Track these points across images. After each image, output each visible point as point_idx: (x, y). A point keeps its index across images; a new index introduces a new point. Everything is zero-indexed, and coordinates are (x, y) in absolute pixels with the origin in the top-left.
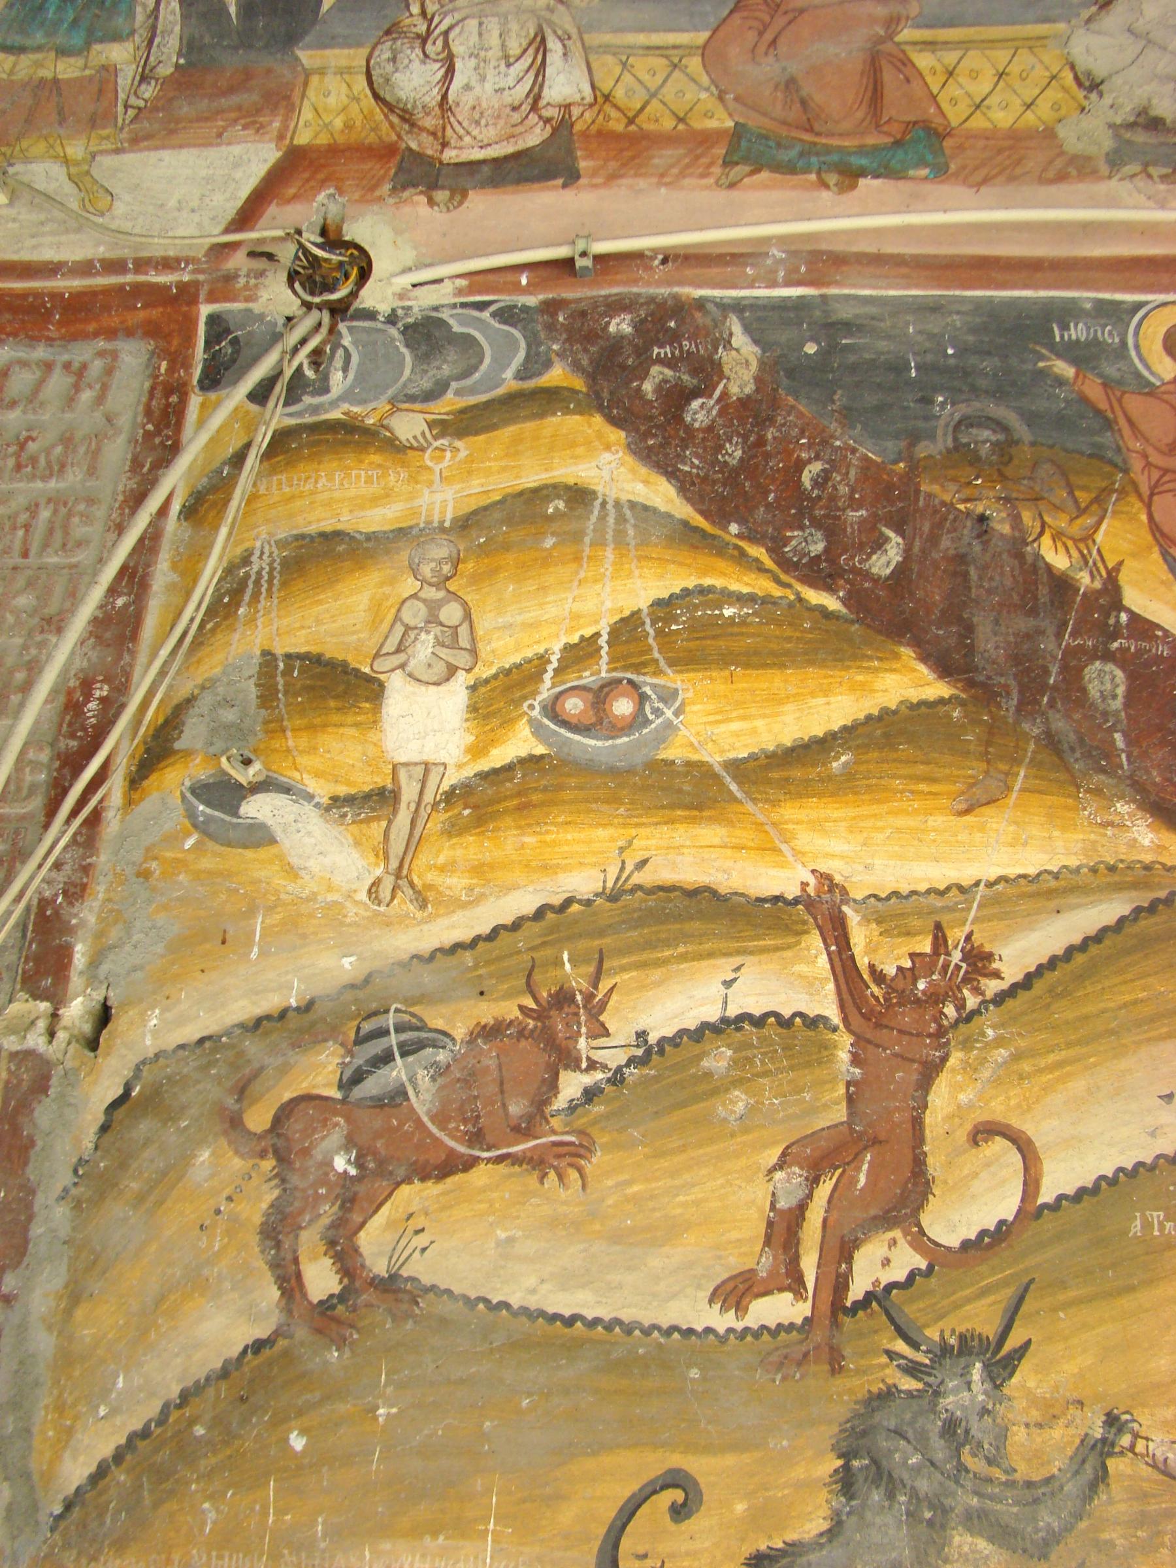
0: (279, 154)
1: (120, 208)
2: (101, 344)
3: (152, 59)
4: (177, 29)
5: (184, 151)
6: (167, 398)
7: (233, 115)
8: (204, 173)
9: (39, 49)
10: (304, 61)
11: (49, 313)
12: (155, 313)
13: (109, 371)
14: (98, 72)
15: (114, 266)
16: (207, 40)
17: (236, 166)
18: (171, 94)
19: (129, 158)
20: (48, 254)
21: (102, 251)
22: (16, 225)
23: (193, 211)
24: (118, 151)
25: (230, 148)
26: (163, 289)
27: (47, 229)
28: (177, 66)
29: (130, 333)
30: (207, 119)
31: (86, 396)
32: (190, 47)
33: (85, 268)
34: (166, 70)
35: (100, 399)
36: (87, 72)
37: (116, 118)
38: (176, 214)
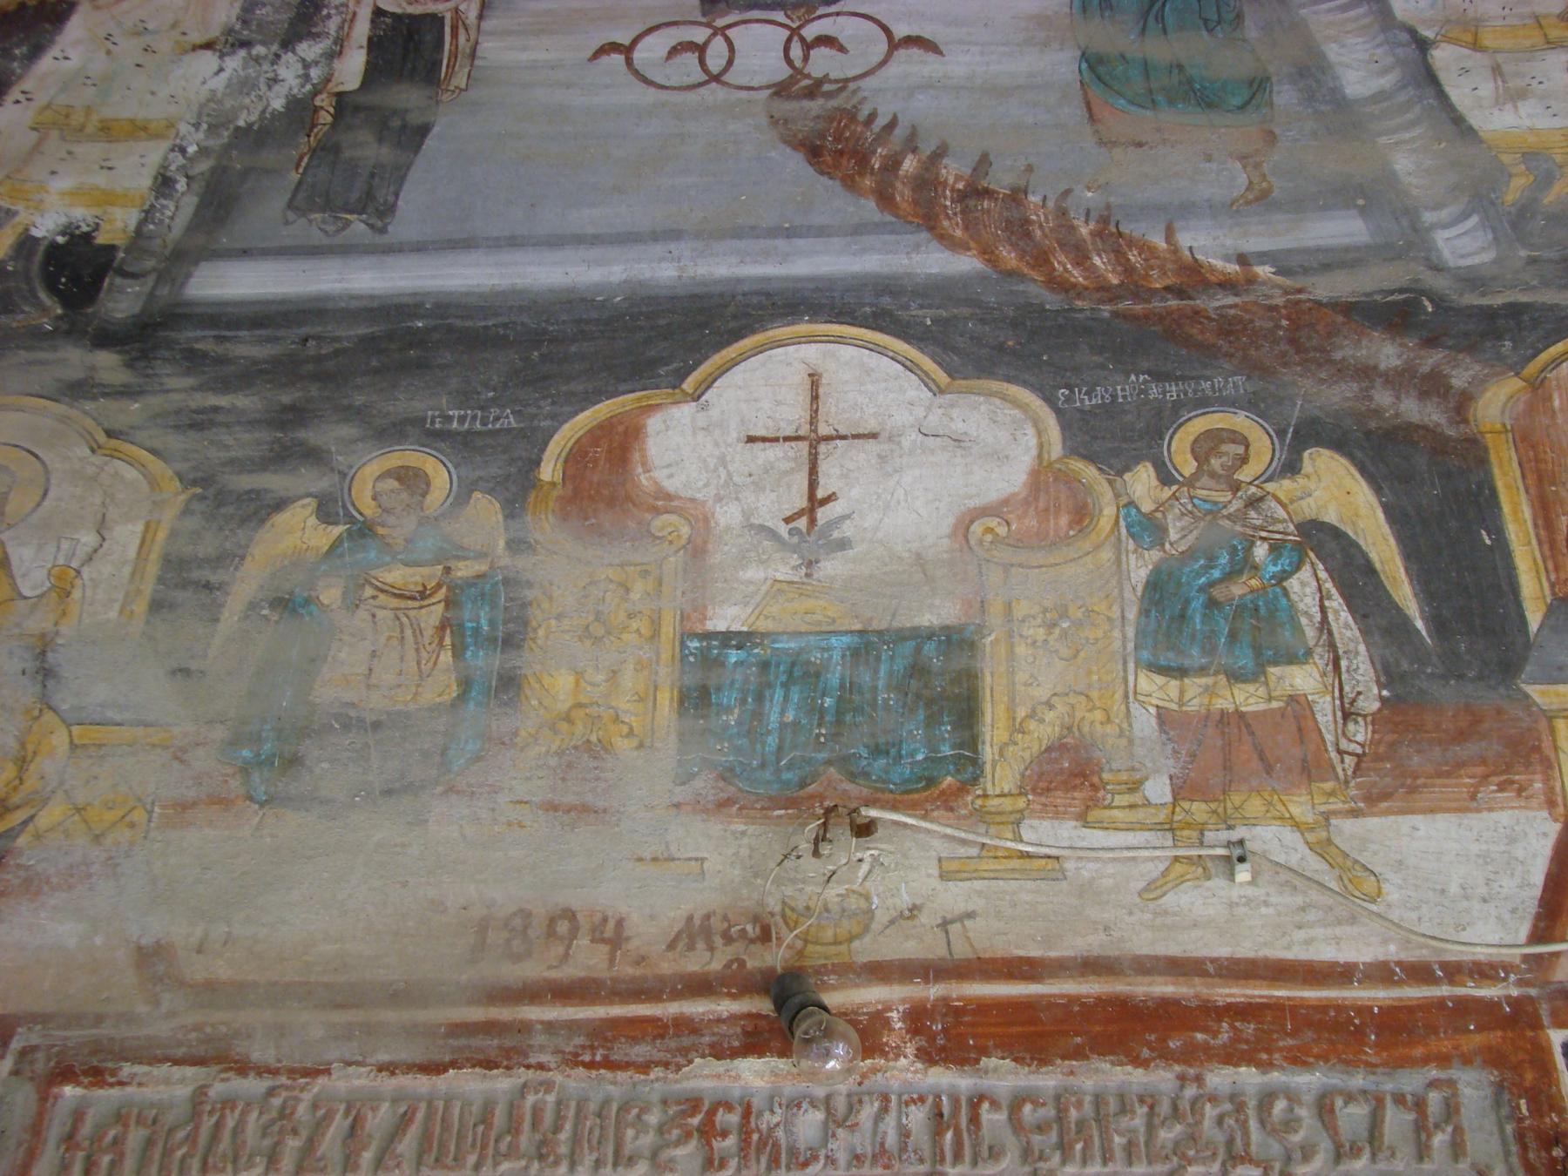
0: (1558, 826)
1: (1392, 894)
2: (1434, 1073)
3: (1347, 688)
4: (1362, 648)
5: (1439, 816)
6: (1549, 1151)
7: (1480, 770)
8: (1475, 848)
9: (1202, 671)
10: (1538, 700)
11: (1359, 1033)
12: (1495, 1037)
13: (1451, 1109)
14: (1288, 704)
15: (1419, 972)
16: (1405, 666)
17: (1512, 840)
18: (1390, 738)
19: (1372, 822)
20: (1326, 953)
21: (1392, 952)
22: (1271, 910)
23: (1485, 901)
24: (1355, 813)
25: (1494, 815)
26: (1490, 1006)
27: (1312, 916)
28: (1381, 698)
29: (1467, 1061)
30: (1448, 775)
31: (1439, 1140)
32: (1388, 675)
33: (1382, 973)
34: (1370, 705)
35: (1457, 1148)
36: (1275, 704)
37: (1334, 768)
38: (1465, 904)
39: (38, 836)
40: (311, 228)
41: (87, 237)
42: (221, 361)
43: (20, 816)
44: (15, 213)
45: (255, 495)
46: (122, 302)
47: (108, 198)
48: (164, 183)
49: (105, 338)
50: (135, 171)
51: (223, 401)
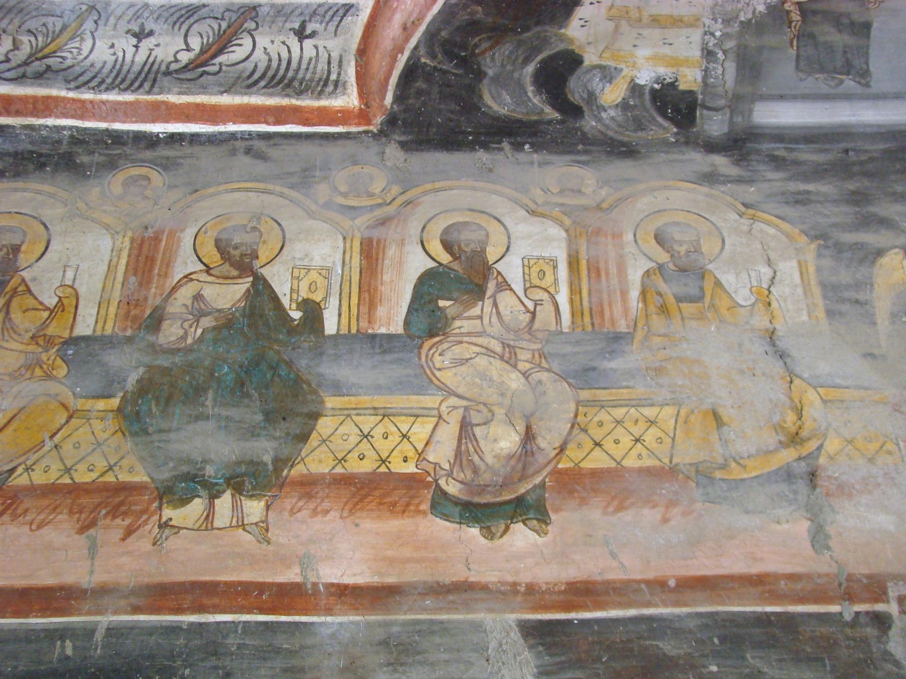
39: (831, 458)
40: (818, 83)
41: (673, 85)
42: (796, 163)
43: (812, 445)
44: (621, 70)
45: (857, 247)
46: (714, 125)
47: (675, 62)
48: (708, 54)
49: (711, 147)
50: (688, 45)
51: (810, 187)
